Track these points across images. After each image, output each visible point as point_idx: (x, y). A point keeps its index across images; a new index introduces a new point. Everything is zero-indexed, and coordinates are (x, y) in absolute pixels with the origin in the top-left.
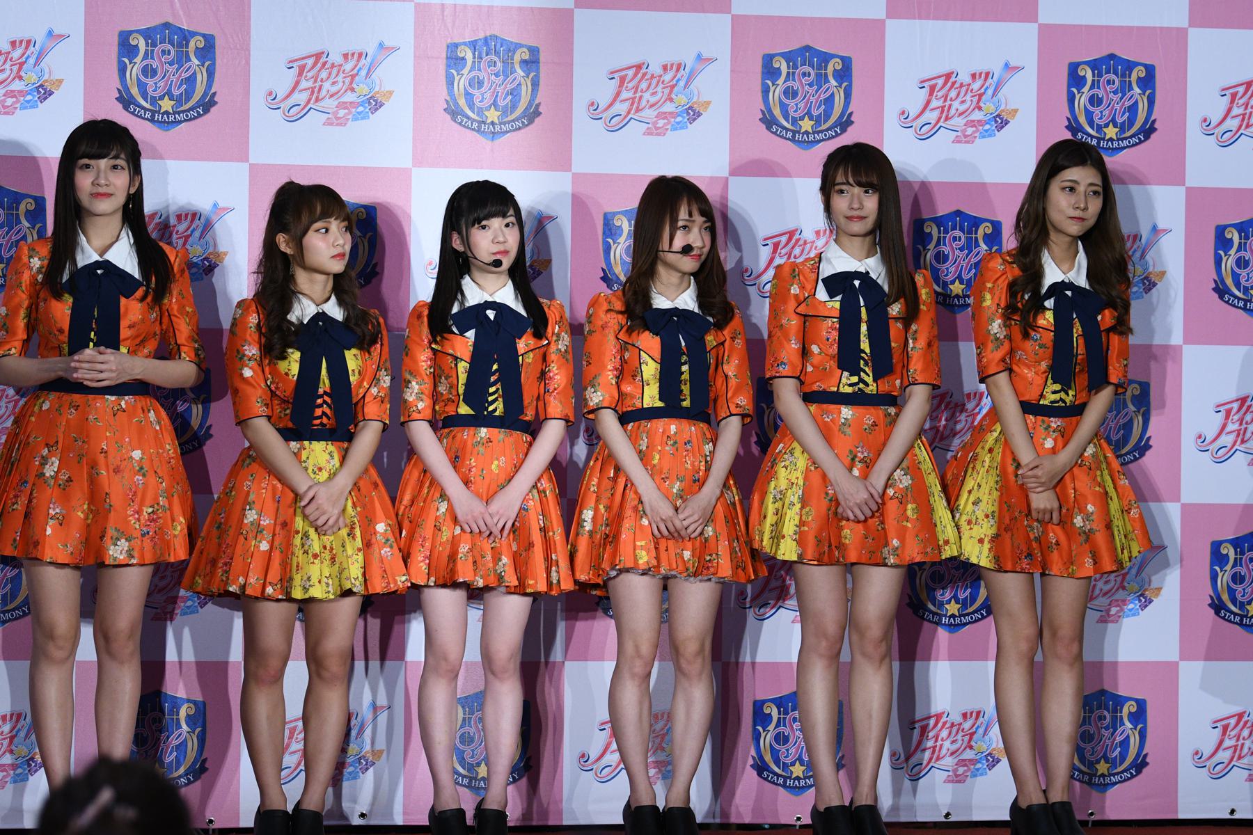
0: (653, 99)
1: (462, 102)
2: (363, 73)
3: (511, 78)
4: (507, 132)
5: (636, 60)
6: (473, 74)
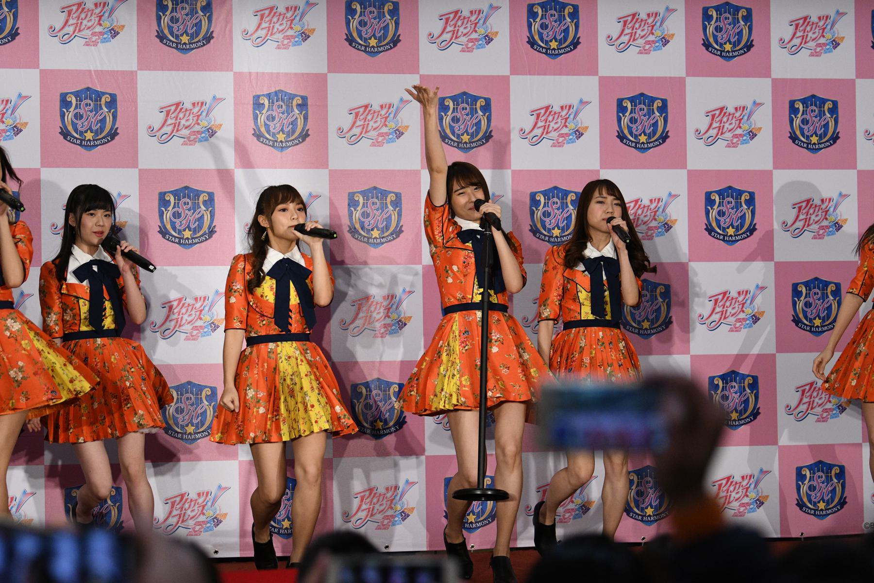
0: (375, 125)
1: (263, 130)
2: (204, 114)
3: (291, 114)
5: (365, 103)
6: (269, 113)
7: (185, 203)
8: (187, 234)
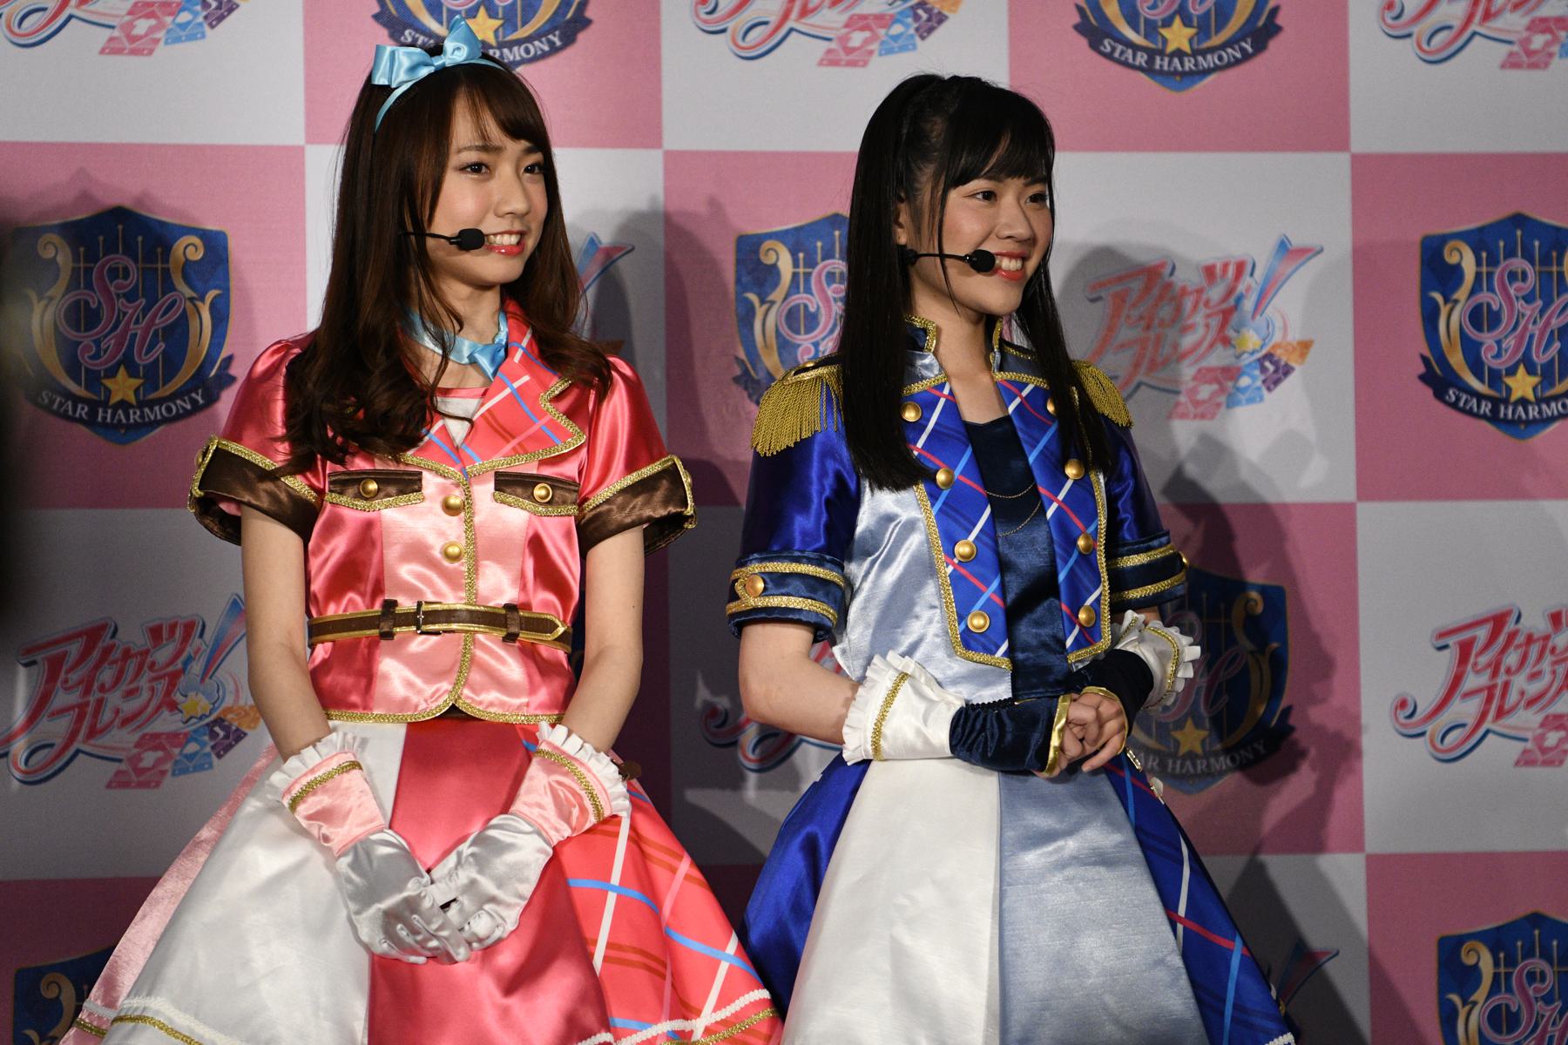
8: (123, 387)
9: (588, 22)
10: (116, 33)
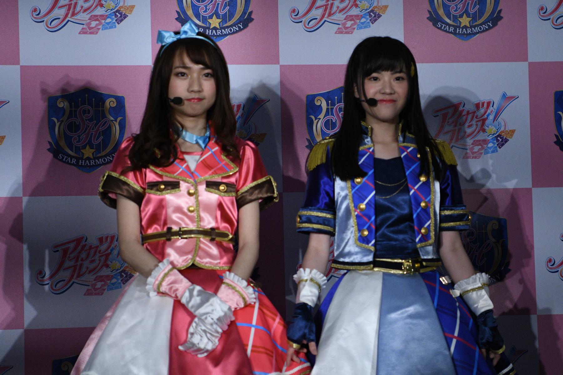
4: (226, 35)
7: (84, 112)
8: (88, 152)
9: (253, 19)
10: (84, 26)
